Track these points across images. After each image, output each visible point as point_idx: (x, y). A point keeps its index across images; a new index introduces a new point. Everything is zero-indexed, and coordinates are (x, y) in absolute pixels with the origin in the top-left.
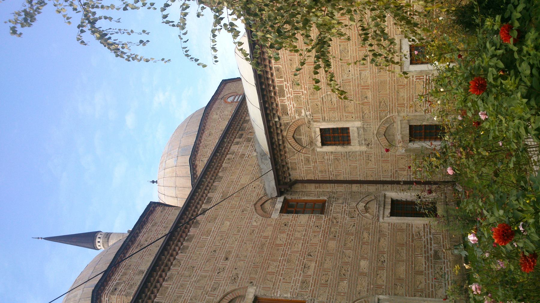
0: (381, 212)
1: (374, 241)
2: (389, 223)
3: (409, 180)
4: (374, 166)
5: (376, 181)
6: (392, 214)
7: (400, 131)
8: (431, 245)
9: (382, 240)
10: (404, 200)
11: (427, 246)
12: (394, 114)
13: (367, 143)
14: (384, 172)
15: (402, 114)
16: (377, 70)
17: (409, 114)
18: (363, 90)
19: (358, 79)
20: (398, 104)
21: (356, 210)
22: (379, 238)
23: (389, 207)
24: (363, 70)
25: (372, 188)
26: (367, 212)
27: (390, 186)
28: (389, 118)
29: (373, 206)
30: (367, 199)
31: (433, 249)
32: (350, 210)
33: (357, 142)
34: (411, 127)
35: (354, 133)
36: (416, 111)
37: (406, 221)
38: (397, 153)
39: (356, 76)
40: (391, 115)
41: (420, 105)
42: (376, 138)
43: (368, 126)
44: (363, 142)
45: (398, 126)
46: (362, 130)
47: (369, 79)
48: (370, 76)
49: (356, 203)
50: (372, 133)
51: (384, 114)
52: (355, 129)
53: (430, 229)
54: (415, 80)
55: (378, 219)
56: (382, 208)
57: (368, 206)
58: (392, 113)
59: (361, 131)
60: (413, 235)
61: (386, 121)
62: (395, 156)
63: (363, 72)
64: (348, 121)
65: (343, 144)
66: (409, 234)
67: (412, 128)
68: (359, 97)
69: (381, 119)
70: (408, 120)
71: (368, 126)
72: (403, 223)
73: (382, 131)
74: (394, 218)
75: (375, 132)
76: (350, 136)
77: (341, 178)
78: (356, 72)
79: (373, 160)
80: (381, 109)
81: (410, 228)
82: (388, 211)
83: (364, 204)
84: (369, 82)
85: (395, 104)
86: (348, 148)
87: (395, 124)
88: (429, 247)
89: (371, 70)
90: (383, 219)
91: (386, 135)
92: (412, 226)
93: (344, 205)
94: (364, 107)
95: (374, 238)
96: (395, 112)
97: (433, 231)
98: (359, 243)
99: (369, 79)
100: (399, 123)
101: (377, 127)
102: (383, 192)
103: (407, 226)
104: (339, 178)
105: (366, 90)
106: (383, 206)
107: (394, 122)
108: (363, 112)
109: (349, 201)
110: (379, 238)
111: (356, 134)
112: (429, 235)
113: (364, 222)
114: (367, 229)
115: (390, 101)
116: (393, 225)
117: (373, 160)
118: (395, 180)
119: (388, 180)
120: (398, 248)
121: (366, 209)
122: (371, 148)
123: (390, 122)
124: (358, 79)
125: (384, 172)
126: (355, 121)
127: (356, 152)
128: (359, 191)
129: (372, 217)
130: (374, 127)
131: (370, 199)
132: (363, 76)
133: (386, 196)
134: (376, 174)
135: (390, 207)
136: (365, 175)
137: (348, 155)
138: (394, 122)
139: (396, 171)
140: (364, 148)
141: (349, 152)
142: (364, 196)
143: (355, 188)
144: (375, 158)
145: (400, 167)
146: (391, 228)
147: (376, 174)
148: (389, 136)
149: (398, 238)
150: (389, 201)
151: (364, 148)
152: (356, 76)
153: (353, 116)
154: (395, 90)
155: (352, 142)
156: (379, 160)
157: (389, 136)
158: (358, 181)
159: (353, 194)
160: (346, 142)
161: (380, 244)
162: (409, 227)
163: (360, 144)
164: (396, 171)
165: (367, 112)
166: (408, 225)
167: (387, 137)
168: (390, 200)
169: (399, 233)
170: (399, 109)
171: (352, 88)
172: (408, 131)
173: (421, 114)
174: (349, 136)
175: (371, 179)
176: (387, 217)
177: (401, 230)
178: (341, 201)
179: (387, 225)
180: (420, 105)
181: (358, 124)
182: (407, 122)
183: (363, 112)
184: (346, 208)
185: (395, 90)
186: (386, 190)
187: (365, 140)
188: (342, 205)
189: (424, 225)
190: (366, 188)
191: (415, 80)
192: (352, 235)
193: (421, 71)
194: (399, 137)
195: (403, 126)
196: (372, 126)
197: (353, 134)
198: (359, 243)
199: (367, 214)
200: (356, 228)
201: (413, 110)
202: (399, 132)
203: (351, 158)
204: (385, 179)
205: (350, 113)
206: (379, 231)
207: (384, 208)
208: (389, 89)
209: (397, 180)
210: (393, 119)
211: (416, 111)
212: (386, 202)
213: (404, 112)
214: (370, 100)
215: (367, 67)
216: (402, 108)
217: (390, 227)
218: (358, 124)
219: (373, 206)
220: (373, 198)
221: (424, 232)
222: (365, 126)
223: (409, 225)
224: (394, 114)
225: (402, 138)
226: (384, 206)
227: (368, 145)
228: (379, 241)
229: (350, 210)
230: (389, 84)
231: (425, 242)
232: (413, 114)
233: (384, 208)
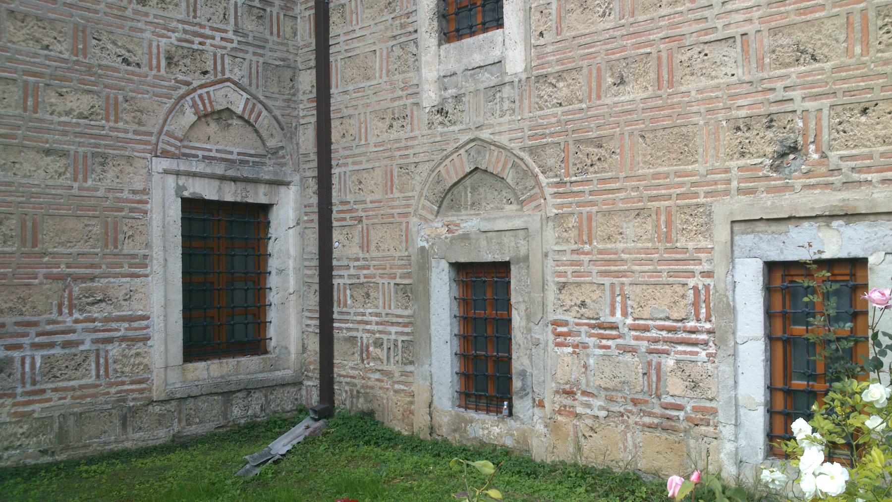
0: (200, 168)
1: (49, 131)
2: (145, 191)
3: (335, 263)
4: (372, 140)
5: (329, 152)
6: (192, 207)
7: (486, 230)
8: (36, 346)
9: (56, 164)
10: (270, 249)
11: (33, 331)
12: (551, 201)
13: (449, 107)
14: (354, 178)
15: (550, 234)
16: (743, 113)
17: (550, 263)
18: (653, 64)
19: (706, 31)
20: (590, 219)
21: (210, 78)
22: (64, 154)
23: (230, 194)
24: (745, 51)
25: (307, 139)
26: (203, 117)
27: (315, 200)
28: (538, 184)
29: (233, 142)
30: (264, 122)
31: (16, 354)
32: (209, 56)
33: (452, 65)
34: (505, 267)
35: (480, 48)
36: (562, 287)
37: (157, 252)
38: (414, 220)
39: (719, 24)
40: (549, 191)
41: (583, 304)
42: (464, 138)
43: (506, 105)
44: (452, 92)
45: (509, 217)
46: (494, 81)
47: (704, 82)
48: (718, 87)
49: (245, 81)
50: (480, 120)
51: (551, 162)
52: (496, 54)
53: (123, 339)
54: (691, 282)
55: (165, 154)
56: (219, 170)
57: (235, 122)
58: (557, 195)
59: (488, 79)
60: (92, 279)
61: (527, 173)
62: (405, 215)
63: (735, 52)
64: (528, 19)
65: (443, 16)
66: (92, 266)
67: (500, 270)
68: (624, 48)
69: (532, 151)
70: (526, 258)
71: (506, 105)
72: (148, 245)
73: (491, 161)
74: (175, 211)
75: (485, 135)
76: (473, 34)
77: (336, 29)
78: (739, 17)
79: (394, 135)
80: (572, 148)
81: (126, 269)
82: (208, 191)
83: (239, 111)
84: (692, 85)
85: (592, 203)
86: (428, 38)
87: (514, 207)
88: (26, 341)
89: (746, 88)
90: (166, 172)
91: (477, 176)
92: (138, 276)
93: (230, 35)
94: (582, 79)
95: (65, 133)
96: (560, 206)
97: (114, 350)
98: (26, 73)
99: (704, 82)
100: (518, 223)
101: (503, 140)
102: (296, 178)
103: (133, 256)
104: (334, 18)
105: (653, 75)
106: (231, 173)
107: (522, 203)
108: (560, 76)
109: (249, 57)
110: (64, 154)
111: (478, 59)
112: (89, 337)
113: (145, 101)
114: (112, 110)
115: (603, 180)
116: (138, 206)
117: (394, 135)
118: (334, 215)
119: (334, 194)
120: (13, 222)
121: (223, 116)
122: (431, 124)
123: (523, 193)
124: (706, 31)
125: (354, 178)
126: (528, 46)
127: (418, 69)
128: (301, 97)
129: (180, 134)
130: (505, 128)
131: (264, 134)
132: (717, 53)
133: (283, 189)
134: (350, 148)
135: (229, 198)
136: (346, 112)
137: (407, 39)
138: (522, 203)
139: (360, 220)
140: (430, 96)
141: (415, 42)
142: (278, 113)
143: (307, 80)
144: (397, 141)
145: (372, 233)
146: (119, 200)
147: (350, 148)
148: (474, 189)
149: (71, 223)
150: (259, 196)
151: (430, 96)
152: (719, 24)
153: (549, 37)
154: (652, 199)
155: (451, 48)
156: (391, 158)
157: (474, 189)
158: (328, 87)
159: (288, 73)
160: (453, 27)
161: (32, 155)
162: (131, 266)
163: (443, 81)
164: (360, 220)
165: (563, 90)
166: (143, 261)
167: (468, 182)
168: (262, 199)
169: (97, 229)
170: (572, 222)
171: (664, 11)
172: (489, 258)
173: (550, 308)
174: (472, 32)
175: (335, 135)
176: (179, 189)
177: (112, 236)
178: (249, 25)
179: (138, 186)
180: (583, 304)
181: (516, 62)
182: (523, 251)
183: (560, 76)
184: (217, 41)
185: (652, 199)
186: (304, 187)
187: (458, 98)
188: (231, 27)
189: (146, 318)
190: (307, 115)
191: (691, 282)
192: (75, 51)
193: (731, 310)
194: (470, 223)
195: (507, 239)
196: (507, 118)
197: (477, 49)
198: (26, 73)
199: (190, 117)
200: (117, 70)
201: (563, 274)
202: (486, 226)
203: (398, 51)
204: (335, 181)
205: (560, 19)
206: (105, 157)
207: (222, 178)
208: (656, 176)
209: (335, 224)
210: (532, 198)
211: (562, 287)
212: (250, 187)
213: (560, 240)
214: (608, 101)
215: (761, 66)
216: (573, 234)
217: (125, 195)
218: (516, 62)
219: (233, 142)
220: (272, 143)
221: (106, 320)
222: (506, 91)
223: (145, 266)
224: (551, 201)
225: (465, 237)
226: (234, 180)
227: (440, 111)
228: (48, 152)
229: (209, 56)
230: (678, 174)
231: (49, 322)
232: (549, 278)
233: (222, 178)
